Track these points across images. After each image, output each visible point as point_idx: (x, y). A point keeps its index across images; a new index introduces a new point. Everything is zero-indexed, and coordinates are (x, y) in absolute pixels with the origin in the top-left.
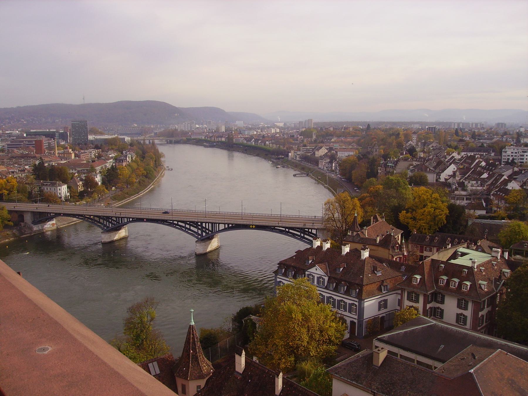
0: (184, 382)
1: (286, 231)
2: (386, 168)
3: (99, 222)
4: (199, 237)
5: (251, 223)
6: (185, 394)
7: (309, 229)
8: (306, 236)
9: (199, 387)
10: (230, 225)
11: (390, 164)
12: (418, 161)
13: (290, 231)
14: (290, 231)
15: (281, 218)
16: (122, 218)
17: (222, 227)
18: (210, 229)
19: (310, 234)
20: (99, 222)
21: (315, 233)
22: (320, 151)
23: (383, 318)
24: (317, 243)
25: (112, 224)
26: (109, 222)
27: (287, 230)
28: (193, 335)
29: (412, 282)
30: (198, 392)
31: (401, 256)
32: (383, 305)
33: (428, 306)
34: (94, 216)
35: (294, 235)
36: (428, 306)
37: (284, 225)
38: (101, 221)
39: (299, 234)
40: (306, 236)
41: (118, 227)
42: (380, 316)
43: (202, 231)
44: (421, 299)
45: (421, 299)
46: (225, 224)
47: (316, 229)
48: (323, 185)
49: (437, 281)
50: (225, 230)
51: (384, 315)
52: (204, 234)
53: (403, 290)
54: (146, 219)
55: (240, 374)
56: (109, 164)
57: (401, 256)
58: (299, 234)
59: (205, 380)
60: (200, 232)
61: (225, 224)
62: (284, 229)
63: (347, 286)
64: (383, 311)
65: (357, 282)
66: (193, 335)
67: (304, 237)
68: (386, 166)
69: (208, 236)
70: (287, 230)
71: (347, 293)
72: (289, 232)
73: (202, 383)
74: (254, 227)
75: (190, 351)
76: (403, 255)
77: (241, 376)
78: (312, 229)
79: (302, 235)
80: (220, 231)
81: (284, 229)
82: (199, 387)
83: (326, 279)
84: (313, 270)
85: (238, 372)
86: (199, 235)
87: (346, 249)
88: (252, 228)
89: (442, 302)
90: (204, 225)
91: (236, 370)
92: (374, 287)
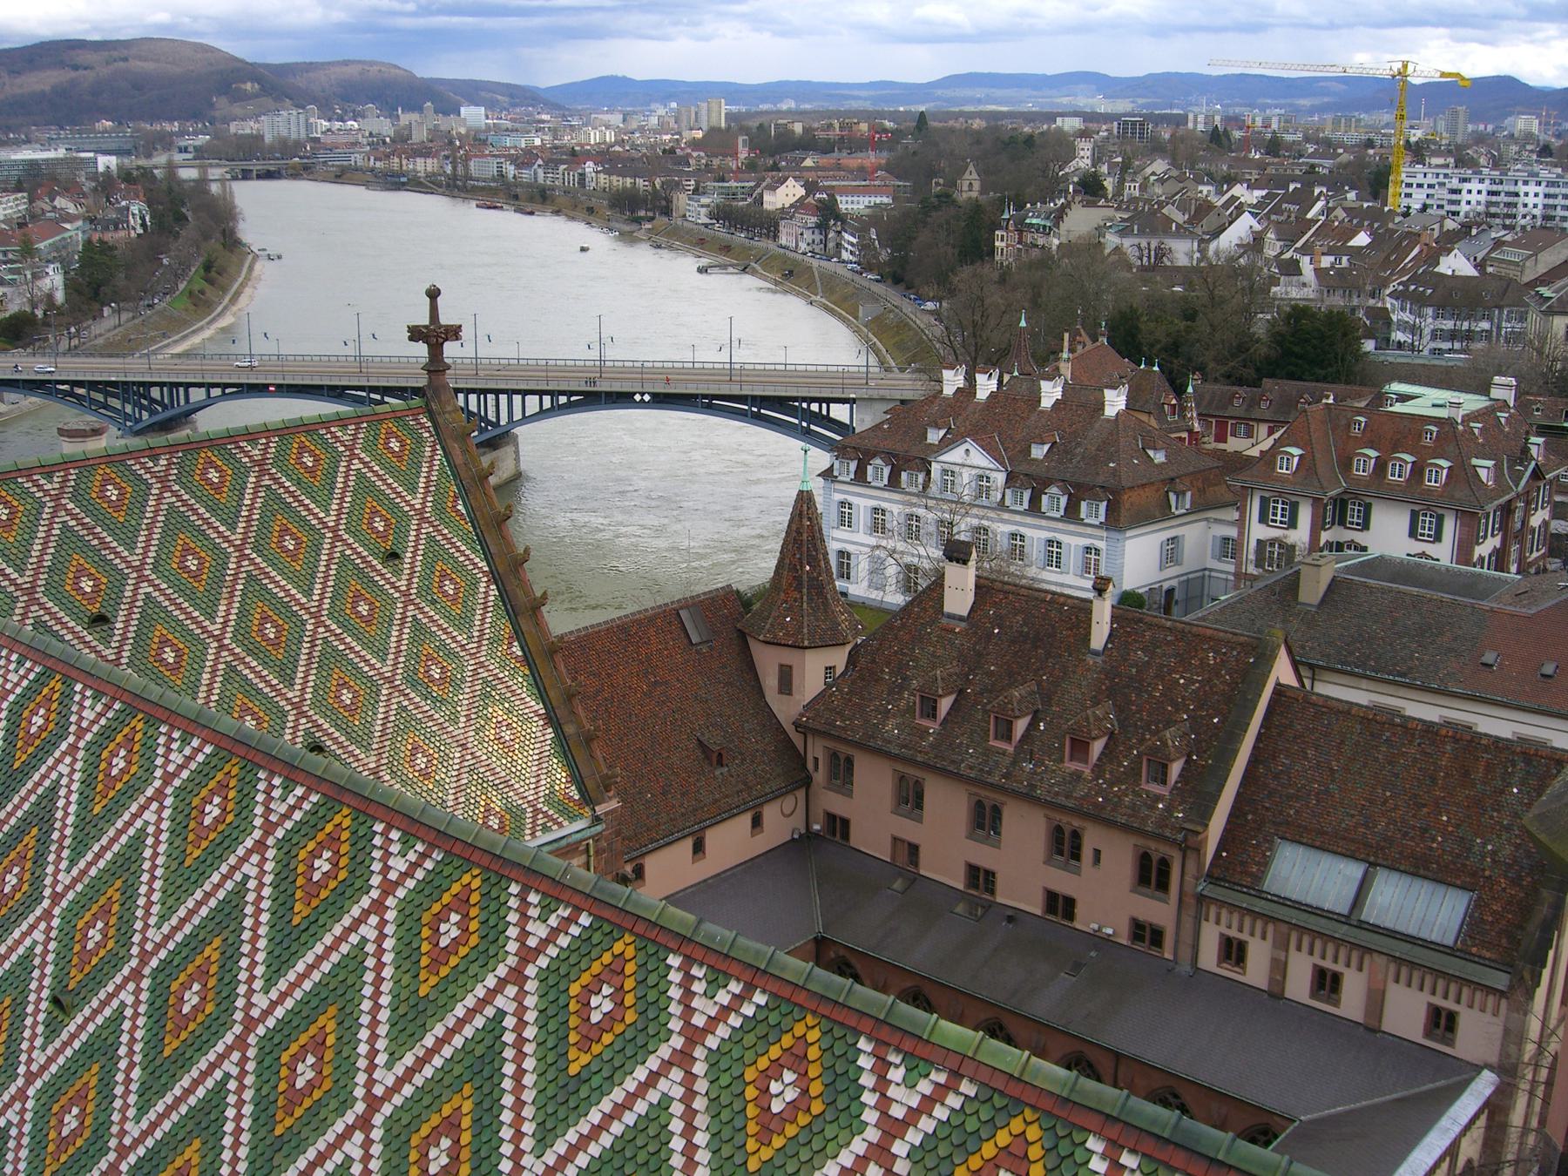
0: (788, 656)
2: (1020, 232)
3: (106, 406)
6: (790, 694)
7: (820, 400)
9: (830, 669)
10: (563, 400)
11: (1034, 221)
12: (1127, 209)
15: (731, 373)
16: (188, 386)
18: (492, 416)
20: (106, 406)
22: (782, 190)
23: (1170, 592)
24: (952, 381)
25: (152, 413)
26: (142, 407)
29: (1274, 468)
30: (828, 686)
31: (1185, 435)
32: (1171, 553)
33: (1325, 537)
34: (93, 385)
36: (1325, 537)
37: (747, 391)
38: (115, 403)
41: (171, 419)
42: (1166, 585)
44: (1305, 515)
45: (1305, 515)
46: (541, 393)
48: (805, 297)
49: (1346, 464)
50: (542, 414)
51: (1174, 583)
53: (1240, 504)
54: (279, 387)
55: (961, 619)
56: (75, 232)
57: (1185, 435)
59: (848, 648)
61: (541, 393)
63: (1070, 495)
64: (1174, 571)
65: (1100, 480)
68: (1022, 227)
71: (1071, 514)
73: (838, 658)
75: (802, 567)
76: (1190, 431)
77: (963, 624)
78: (829, 401)
80: (526, 419)
82: (830, 669)
83: (1000, 478)
84: (955, 455)
85: (951, 616)
87: (1051, 392)
88: (642, 404)
89: (1365, 526)
91: (947, 609)
92: (1147, 497)
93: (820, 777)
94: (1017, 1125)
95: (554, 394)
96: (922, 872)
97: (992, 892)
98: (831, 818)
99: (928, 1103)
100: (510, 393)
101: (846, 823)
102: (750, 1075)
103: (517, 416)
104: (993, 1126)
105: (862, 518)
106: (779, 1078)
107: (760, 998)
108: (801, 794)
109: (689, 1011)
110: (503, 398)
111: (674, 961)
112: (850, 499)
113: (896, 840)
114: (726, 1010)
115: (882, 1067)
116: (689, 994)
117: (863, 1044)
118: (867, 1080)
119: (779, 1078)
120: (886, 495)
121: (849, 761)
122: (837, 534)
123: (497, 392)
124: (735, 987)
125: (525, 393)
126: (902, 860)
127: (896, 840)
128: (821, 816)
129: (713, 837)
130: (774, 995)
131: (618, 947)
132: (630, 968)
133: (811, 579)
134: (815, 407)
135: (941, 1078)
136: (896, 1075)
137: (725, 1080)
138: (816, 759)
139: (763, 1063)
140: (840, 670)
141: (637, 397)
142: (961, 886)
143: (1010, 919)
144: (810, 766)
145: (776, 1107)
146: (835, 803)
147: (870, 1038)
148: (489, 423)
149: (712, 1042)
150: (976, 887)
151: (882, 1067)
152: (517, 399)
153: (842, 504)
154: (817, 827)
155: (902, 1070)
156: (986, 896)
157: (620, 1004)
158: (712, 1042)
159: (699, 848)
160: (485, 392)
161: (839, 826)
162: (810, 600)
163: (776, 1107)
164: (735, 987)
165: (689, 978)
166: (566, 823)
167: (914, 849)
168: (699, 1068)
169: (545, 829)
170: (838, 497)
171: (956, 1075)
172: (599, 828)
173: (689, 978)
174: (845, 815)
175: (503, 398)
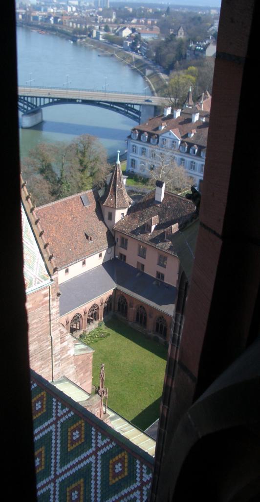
1: (112, 106)
4: (25, 111)
5: (77, 98)
7: (131, 104)
8: (129, 112)
9: (123, 214)
10: (56, 100)
13: (115, 106)
14: (115, 106)
17: (47, 101)
18: (35, 103)
19: (132, 109)
21: (138, 109)
27: (112, 105)
28: (119, 172)
35: (118, 111)
37: (110, 100)
39: (123, 109)
40: (129, 112)
43: (28, 106)
47: (140, 105)
50: (50, 104)
52: (29, 109)
58: (123, 109)
60: (26, 107)
61: (49, 98)
62: (109, 104)
66: (119, 172)
67: (127, 113)
69: (33, 110)
70: (112, 105)
72: (113, 107)
73: (125, 211)
74: (80, 101)
78: (134, 104)
79: (126, 110)
81: (109, 104)
86: (25, 109)
88: (79, 103)
90: (26, 99)
93: (119, 243)
94: (123, 454)
95: (53, 99)
96: (145, 272)
97: (163, 280)
98: (121, 255)
99: (105, 445)
100: (40, 98)
101: (125, 257)
102: (69, 430)
103: (42, 104)
104: (118, 454)
105: (139, 150)
106: (75, 432)
107: (72, 413)
108: (113, 248)
109: (57, 413)
110: (38, 99)
111: (54, 400)
112: (136, 145)
113: (138, 263)
114: (65, 414)
115: (97, 435)
116: (57, 409)
117: (93, 429)
118: (93, 437)
119: (75, 432)
120: (146, 144)
121: (127, 240)
122: (131, 154)
123: (36, 97)
124: (67, 409)
125: (44, 98)
126: (140, 268)
127: (138, 263)
128: (118, 254)
129: (87, 260)
130: (75, 414)
131: (42, 394)
132: (45, 399)
133: (119, 189)
134: (129, 105)
135: (109, 440)
136: (99, 437)
137: (64, 430)
138: (118, 239)
139: (72, 428)
140: (125, 214)
141: (77, 101)
142: (155, 277)
143: (167, 288)
144: (116, 240)
145: (74, 438)
146: (123, 251)
147: (95, 428)
148: (34, 105)
149: (62, 420)
150: (159, 277)
151: (97, 435)
152: (42, 99)
153: (133, 146)
154: (117, 257)
155: (101, 437)
156: (161, 280)
157: (42, 407)
158: (62, 420)
159: (84, 263)
160: (33, 97)
161: (123, 257)
162: (118, 194)
163: (74, 438)
164: (67, 409)
165: (57, 405)
166: (43, 281)
167: (143, 266)
168: (59, 426)
169: (38, 283)
170: (132, 144)
171: (111, 441)
172: (52, 282)
173: (57, 405)
174: (125, 254)
175: (38, 99)
